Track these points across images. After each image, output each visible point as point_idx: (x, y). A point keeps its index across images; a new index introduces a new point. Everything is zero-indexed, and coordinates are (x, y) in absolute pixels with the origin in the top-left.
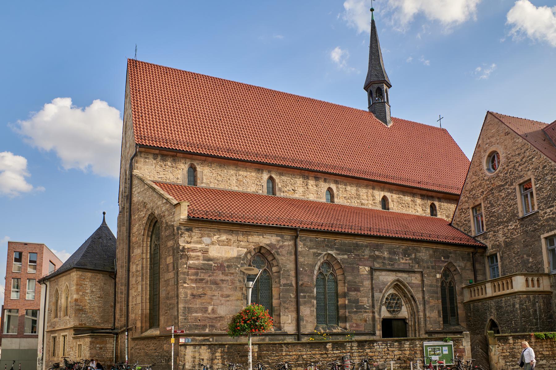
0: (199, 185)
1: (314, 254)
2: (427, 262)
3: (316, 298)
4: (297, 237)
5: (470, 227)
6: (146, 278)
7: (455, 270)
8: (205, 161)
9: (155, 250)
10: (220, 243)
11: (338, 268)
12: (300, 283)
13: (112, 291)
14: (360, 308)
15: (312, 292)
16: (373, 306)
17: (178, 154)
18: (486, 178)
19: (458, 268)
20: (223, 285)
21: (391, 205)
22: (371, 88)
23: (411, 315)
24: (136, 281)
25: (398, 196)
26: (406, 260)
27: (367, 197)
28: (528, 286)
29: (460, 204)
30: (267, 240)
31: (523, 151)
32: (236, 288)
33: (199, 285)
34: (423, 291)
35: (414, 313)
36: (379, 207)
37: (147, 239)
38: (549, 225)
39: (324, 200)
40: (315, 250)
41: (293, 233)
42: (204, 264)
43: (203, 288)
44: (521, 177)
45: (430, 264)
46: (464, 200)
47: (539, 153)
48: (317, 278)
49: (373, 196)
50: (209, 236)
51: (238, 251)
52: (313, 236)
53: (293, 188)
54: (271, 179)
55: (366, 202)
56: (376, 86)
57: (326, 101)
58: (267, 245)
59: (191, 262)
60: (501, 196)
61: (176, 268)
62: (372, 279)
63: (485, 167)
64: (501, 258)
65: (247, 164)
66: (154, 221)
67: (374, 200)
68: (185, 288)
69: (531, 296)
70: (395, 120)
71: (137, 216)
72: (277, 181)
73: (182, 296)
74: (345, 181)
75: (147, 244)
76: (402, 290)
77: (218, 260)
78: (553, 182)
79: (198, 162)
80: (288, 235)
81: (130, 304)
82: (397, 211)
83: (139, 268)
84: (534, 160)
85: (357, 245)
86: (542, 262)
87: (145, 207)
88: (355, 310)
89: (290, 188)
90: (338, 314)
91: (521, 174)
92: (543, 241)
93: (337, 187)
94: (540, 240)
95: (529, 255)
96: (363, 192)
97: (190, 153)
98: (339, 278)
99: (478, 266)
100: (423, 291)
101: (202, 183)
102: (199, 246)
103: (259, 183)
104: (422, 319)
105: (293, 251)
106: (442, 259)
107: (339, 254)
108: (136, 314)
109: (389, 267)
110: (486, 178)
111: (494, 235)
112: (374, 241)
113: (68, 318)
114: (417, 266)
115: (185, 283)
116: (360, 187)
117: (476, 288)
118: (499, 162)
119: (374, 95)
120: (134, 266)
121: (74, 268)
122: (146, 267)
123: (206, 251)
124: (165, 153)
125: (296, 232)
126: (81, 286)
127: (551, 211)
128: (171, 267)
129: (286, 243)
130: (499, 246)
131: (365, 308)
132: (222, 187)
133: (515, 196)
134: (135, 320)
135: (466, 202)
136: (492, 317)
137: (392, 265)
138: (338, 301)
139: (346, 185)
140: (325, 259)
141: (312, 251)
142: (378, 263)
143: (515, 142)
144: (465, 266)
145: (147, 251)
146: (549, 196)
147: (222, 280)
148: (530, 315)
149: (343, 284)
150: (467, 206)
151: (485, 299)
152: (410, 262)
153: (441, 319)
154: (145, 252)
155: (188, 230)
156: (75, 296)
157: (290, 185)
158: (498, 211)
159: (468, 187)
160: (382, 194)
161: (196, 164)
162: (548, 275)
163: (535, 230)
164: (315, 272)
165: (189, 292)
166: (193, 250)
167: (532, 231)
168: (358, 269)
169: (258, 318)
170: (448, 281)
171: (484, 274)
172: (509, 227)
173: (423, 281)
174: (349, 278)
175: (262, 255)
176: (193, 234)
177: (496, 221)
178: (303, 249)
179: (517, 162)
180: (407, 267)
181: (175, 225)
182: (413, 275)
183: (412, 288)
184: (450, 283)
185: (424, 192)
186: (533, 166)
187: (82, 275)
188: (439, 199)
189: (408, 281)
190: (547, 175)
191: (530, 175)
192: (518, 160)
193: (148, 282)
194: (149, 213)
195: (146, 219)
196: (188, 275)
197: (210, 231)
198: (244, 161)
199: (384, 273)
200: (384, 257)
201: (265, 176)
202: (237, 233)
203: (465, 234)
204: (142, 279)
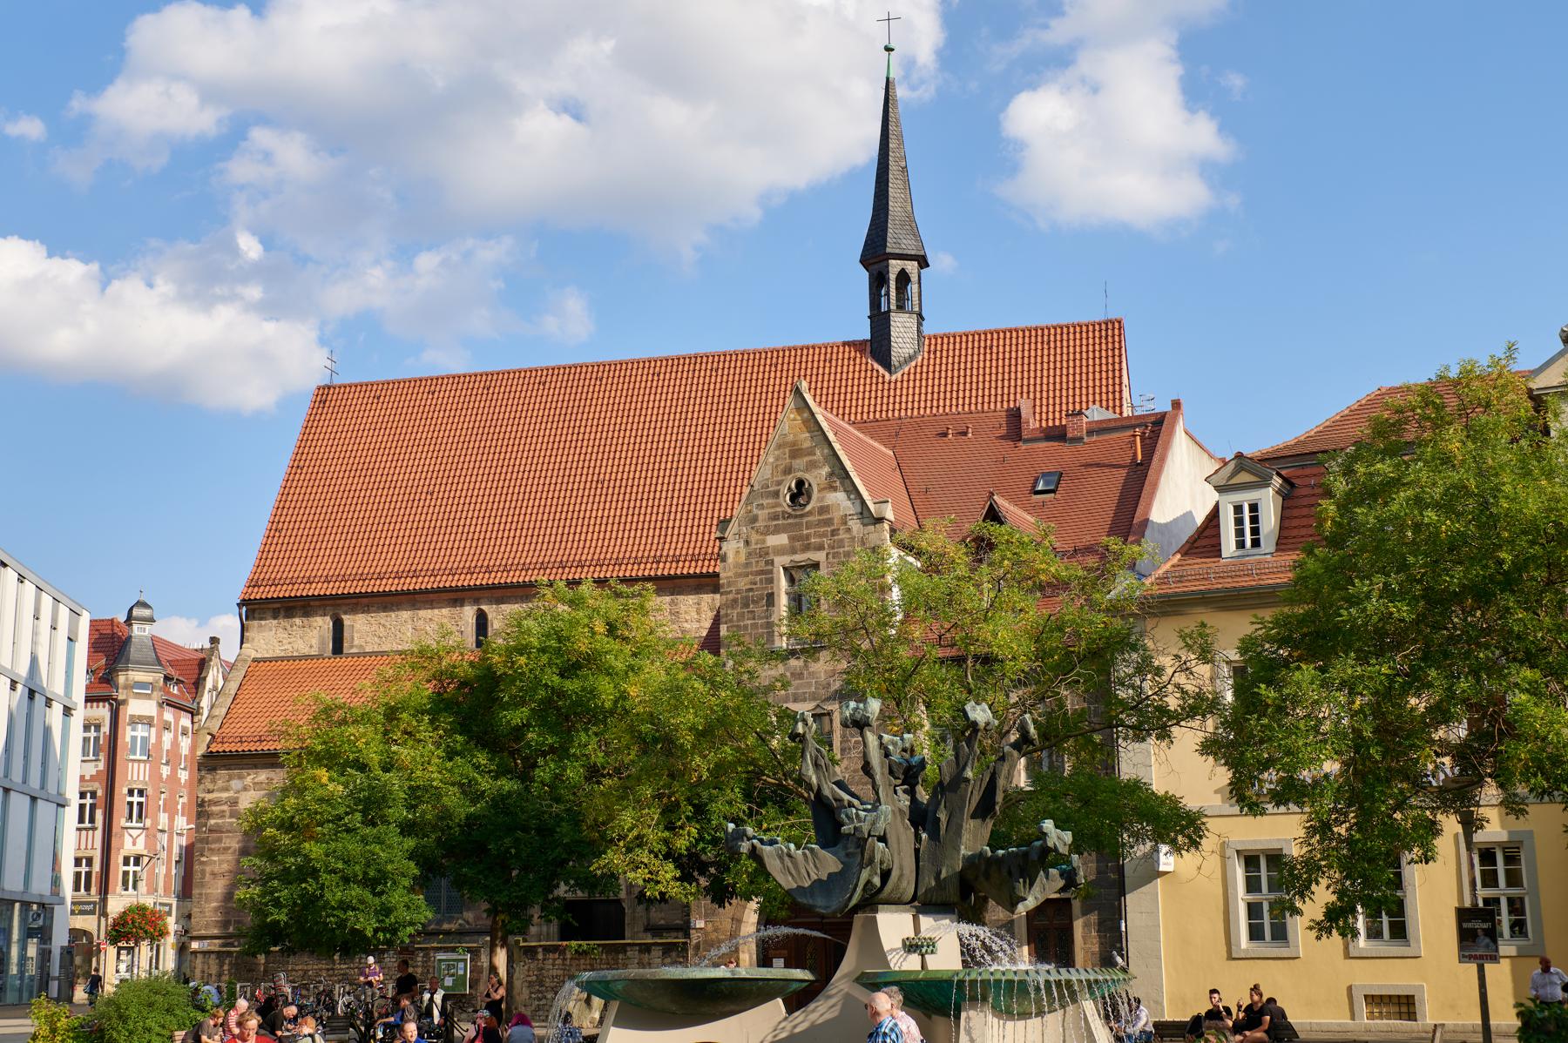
59: (212, 822)
102: (225, 795)
166: (216, 803)
201: (469, 612)
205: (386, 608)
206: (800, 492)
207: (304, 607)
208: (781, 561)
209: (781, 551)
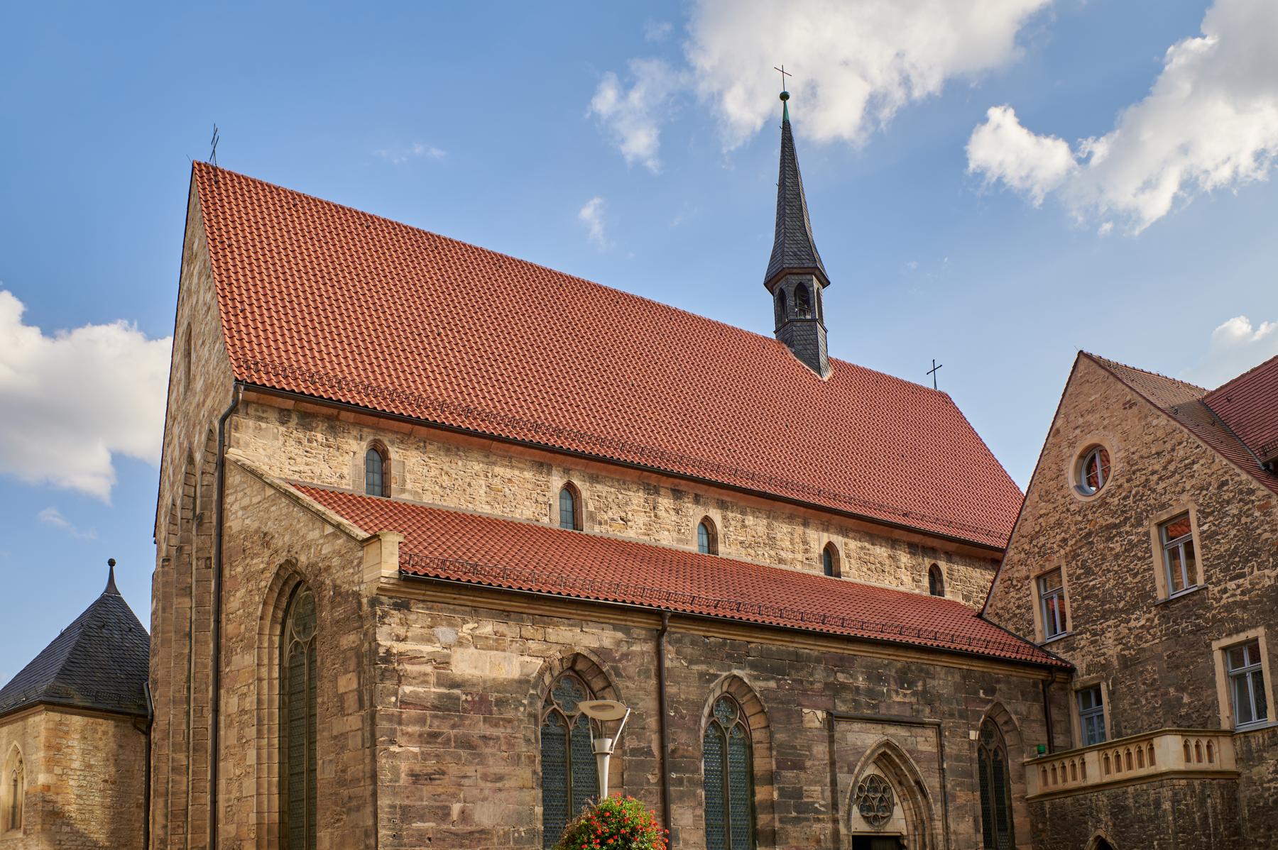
0: (395, 496)
1: (702, 675)
2: (948, 701)
3: (705, 785)
4: (661, 633)
5: (1031, 622)
6: (269, 730)
7: (1006, 723)
8: (409, 435)
9: (292, 657)
10: (478, 641)
11: (753, 711)
12: (671, 746)
13: (140, 765)
14: (805, 811)
15: (698, 770)
16: (835, 806)
17: (344, 414)
18: (1073, 507)
19: (1014, 717)
20: (488, 751)
21: (845, 567)
22: (782, 284)
23: (915, 828)
24: (239, 739)
25: (859, 544)
26: (905, 695)
27: (792, 544)
28: (1188, 759)
29: (1004, 567)
30: (592, 638)
31: (1168, 446)
32: (519, 756)
33: (427, 749)
34: (942, 770)
35: (921, 824)
36: (818, 571)
37: (272, 628)
38: (1233, 619)
39: (693, 548)
40: (703, 667)
41: (652, 623)
42: (441, 696)
43: (437, 756)
44: (1163, 506)
45: (955, 706)
46: (1016, 558)
47: (1210, 451)
48: (707, 736)
49: (805, 542)
50: (451, 625)
51: (522, 665)
52: (697, 632)
53: (623, 515)
54: (570, 489)
55: (790, 556)
56: (795, 280)
57: (681, 308)
58: (593, 651)
59: (407, 689)
60: (1112, 549)
61: (367, 703)
62: (831, 740)
63: (1072, 483)
64: (1112, 694)
65: (515, 447)
66: (292, 583)
67: (806, 551)
68: (394, 755)
69: (1196, 783)
70: (838, 365)
71: (240, 569)
72: (585, 494)
73: (385, 777)
74: (742, 504)
75: (271, 642)
76: (896, 766)
77: (474, 685)
78: (1244, 520)
79: (394, 437)
80: (640, 627)
81: (221, 797)
82: (857, 581)
83: (250, 703)
84: (1195, 467)
85: (797, 657)
86: (1214, 705)
87: (267, 545)
88: (794, 814)
89: (614, 513)
90: (755, 824)
91: (1164, 499)
92: (1218, 656)
93: (724, 518)
94: (1211, 653)
95: (1182, 689)
96: (783, 530)
97: (374, 413)
98: (757, 736)
99: (1055, 714)
100: (942, 770)
101: (403, 491)
102: (427, 649)
103: (541, 499)
104: (940, 838)
105: (653, 668)
106: (982, 695)
107: (756, 678)
108: (239, 825)
109: (868, 712)
110: (1073, 507)
111: (1092, 642)
112: (835, 649)
113: (20, 835)
114: (927, 710)
115: (393, 742)
116: (775, 518)
117: (1058, 765)
118: (1106, 472)
119: (790, 302)
120: (234, 700)
121: (41, 702)
122: (270, 701)
123: (443, 663)
124: (310, 407)
125: (660, 621)
126: (59, 750)
127: (1238, 586)
128: (351, 702)
129: (636, 648)
130: (1104, 667)
131: (817, 811)
132: (452, 502)
133: (1148, 550)
134: (239, 839)
135: (1022, 563)
136: (1101, 833)
137: (875, 707)
138: (753, 794)
139: (743, 513)
140: (725, 689)
141: (695, 667)
142: (845, 701)
143: (1148, 425)
144: (1029, 713)
145: (270, 659)
146: (1234, 552)
147: (485, 738)
148: (1195, 828)
149: (766, 753)
150: (1024, 573)
151: (1085, 788)
152: (914, 700)
153: (980, 837)
154: (266, 661)
155: (399, 606)
156: (42, 779)
157: (615, 507)
158: (1103, 585)
159: (1028, 527)
160: (826, 538)
161: (386, 443)
162: (1231, 734)
163: (1198, 630)
165: (404, 767)
166: (413, 659)
167: (1190, 632)
168: (800, 715)
169: (634, 831)
170: (992, 746)
171: (1068, 732)
172: (1133, 624)
173: (941, 746)
174: (780, 736)
175: (580, 674)
176: (412, 617)
177: (1097, 610)
178: (676, 663)
179: (1154, 473)
180: (907, 713)
181: (363, 593)
182: (919, 731)
183: (918, 762)
184: (996, 754)
185: (916, 539)
186: (1194, 481)
187: (60, 723)
188: (949, 556)
189: (910, 747)
190: (1228, 503)
191: (1187, 503)
192: (1156, 467)
193: (276, 741)
194: (281, 559)
195: (269, 576)
196: (400, 723)
197: (454, 611)
198: (506, 440)
199: (856, 726)
200: (857, 688)
202: (518, 617)
203: (1019, 638)
204: (259, 731)
205: (450, 449)
207: (329, 418)
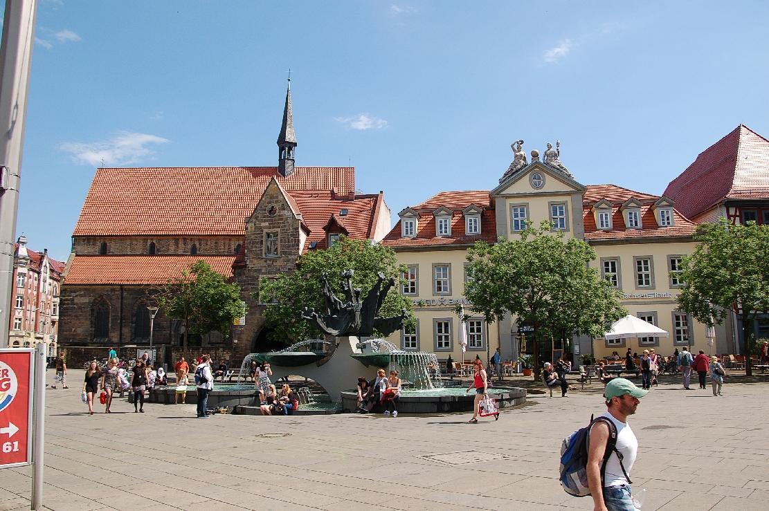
10: (81, 296)
123: (73, 300)
164: (136, 308)
166: (67, 300)
206: (272, 211)
208: (265, 231)
209: (266, 227)
